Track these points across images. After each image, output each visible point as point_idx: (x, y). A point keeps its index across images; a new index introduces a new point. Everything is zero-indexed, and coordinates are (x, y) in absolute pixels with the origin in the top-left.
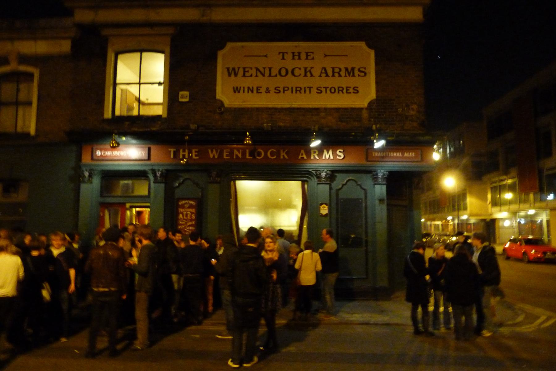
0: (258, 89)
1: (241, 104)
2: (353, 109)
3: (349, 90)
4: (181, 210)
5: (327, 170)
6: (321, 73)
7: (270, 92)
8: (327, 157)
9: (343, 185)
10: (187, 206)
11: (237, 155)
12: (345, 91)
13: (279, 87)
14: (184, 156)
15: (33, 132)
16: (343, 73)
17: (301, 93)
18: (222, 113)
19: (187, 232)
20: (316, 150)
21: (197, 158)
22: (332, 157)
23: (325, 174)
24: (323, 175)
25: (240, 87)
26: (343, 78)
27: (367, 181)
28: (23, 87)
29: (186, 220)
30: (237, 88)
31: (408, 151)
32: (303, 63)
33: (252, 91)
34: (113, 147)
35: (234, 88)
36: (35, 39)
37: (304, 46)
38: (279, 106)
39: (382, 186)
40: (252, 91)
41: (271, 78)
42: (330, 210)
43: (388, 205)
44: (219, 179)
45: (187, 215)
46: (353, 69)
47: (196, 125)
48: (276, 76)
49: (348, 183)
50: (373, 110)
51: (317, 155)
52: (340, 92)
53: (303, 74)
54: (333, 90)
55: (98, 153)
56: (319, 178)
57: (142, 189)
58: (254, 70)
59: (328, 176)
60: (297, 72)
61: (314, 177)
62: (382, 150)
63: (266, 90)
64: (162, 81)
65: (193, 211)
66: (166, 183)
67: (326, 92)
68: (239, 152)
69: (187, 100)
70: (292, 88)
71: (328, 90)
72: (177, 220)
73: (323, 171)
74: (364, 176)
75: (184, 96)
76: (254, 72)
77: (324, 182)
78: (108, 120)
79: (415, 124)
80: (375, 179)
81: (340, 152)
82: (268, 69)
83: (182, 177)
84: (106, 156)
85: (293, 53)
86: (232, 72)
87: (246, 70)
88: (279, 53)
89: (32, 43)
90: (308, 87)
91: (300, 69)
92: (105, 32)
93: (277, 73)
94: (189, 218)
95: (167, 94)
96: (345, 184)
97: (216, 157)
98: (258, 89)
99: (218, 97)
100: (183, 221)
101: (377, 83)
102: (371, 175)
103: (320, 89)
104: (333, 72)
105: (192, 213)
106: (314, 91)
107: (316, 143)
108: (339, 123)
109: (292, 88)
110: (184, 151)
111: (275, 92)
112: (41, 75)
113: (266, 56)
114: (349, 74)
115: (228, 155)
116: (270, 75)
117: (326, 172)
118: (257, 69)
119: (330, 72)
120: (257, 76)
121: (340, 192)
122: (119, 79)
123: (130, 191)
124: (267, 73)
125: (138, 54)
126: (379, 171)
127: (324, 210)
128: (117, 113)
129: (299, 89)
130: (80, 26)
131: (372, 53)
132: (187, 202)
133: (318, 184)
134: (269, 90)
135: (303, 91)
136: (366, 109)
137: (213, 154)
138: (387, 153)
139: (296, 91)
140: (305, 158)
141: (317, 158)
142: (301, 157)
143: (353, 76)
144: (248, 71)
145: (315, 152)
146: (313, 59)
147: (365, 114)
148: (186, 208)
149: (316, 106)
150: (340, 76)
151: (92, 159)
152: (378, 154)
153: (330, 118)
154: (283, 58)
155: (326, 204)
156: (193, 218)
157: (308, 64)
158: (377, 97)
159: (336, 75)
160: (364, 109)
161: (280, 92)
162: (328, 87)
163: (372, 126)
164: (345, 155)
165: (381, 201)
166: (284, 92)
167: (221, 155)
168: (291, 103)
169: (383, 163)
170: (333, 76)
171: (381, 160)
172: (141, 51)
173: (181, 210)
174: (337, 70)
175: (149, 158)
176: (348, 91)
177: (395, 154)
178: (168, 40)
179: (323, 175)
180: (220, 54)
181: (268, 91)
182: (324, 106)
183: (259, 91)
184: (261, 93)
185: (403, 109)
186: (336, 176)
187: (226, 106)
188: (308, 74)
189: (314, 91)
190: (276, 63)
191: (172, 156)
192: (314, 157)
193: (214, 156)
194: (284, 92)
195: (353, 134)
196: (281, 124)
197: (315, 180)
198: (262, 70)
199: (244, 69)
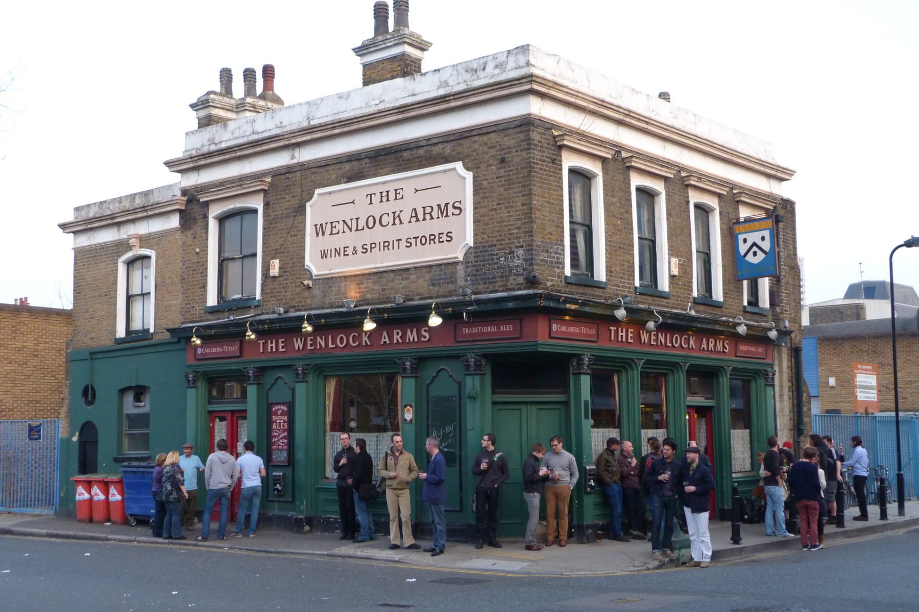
4: (274, 418)
6: (411, 217)
9: (434, 378)
10: (280, 412)
13: (366, 245)
16: (435, 214)
22: (416, 340)
29: (279, 430)
32: (391, 206)
33: (339, 254)
42: (416, 414)
45: (280, 423)
46: (447, 204)
51: (401, 337)
52: (432, 242)
54: (423, 242)
65: (285, 418)
71: (418, 240)
76: (340, 227)
81: (425, 331)
85: (381, 193)
86: (320, 230)
88: (367, 195)
90: (397, 240)
91: (388, 214)
100: (276, 432)
101: (476, 221)
104: (425, 214)
105: (284, 422)
106: (403, 243)
110: (272, 343)
113: (353, 202)
114: (442, 213)
116: (357, 230)
118: (344, 221)
119: (421, 217)
120: (344, 232)
121: (431, 387)
124: (354, 228)
126: (469, 357)
129: (386, 244)
131: (469, 176)
132: (277, 407)
135: (391, 247)
140: (388, 342)
141: (400, 341)
143: (447, 216)
144: (335, 227)
146: (402, 198)
150: (432, 218)
153: (421, 281)
154: (371, 203)
155: (411, 406)
158: (475, 243)
159: (428, 217)
162: (418, 237)
166: (371, 252)
170: (424, 219)
173: (274, 418)
174: (428, 210)
184: (348, 255)
185: (506, 259)
188: (397, 221)
189: (403, 243)
194: (371, 252)
198: (349, 222)
199: (331, 223)
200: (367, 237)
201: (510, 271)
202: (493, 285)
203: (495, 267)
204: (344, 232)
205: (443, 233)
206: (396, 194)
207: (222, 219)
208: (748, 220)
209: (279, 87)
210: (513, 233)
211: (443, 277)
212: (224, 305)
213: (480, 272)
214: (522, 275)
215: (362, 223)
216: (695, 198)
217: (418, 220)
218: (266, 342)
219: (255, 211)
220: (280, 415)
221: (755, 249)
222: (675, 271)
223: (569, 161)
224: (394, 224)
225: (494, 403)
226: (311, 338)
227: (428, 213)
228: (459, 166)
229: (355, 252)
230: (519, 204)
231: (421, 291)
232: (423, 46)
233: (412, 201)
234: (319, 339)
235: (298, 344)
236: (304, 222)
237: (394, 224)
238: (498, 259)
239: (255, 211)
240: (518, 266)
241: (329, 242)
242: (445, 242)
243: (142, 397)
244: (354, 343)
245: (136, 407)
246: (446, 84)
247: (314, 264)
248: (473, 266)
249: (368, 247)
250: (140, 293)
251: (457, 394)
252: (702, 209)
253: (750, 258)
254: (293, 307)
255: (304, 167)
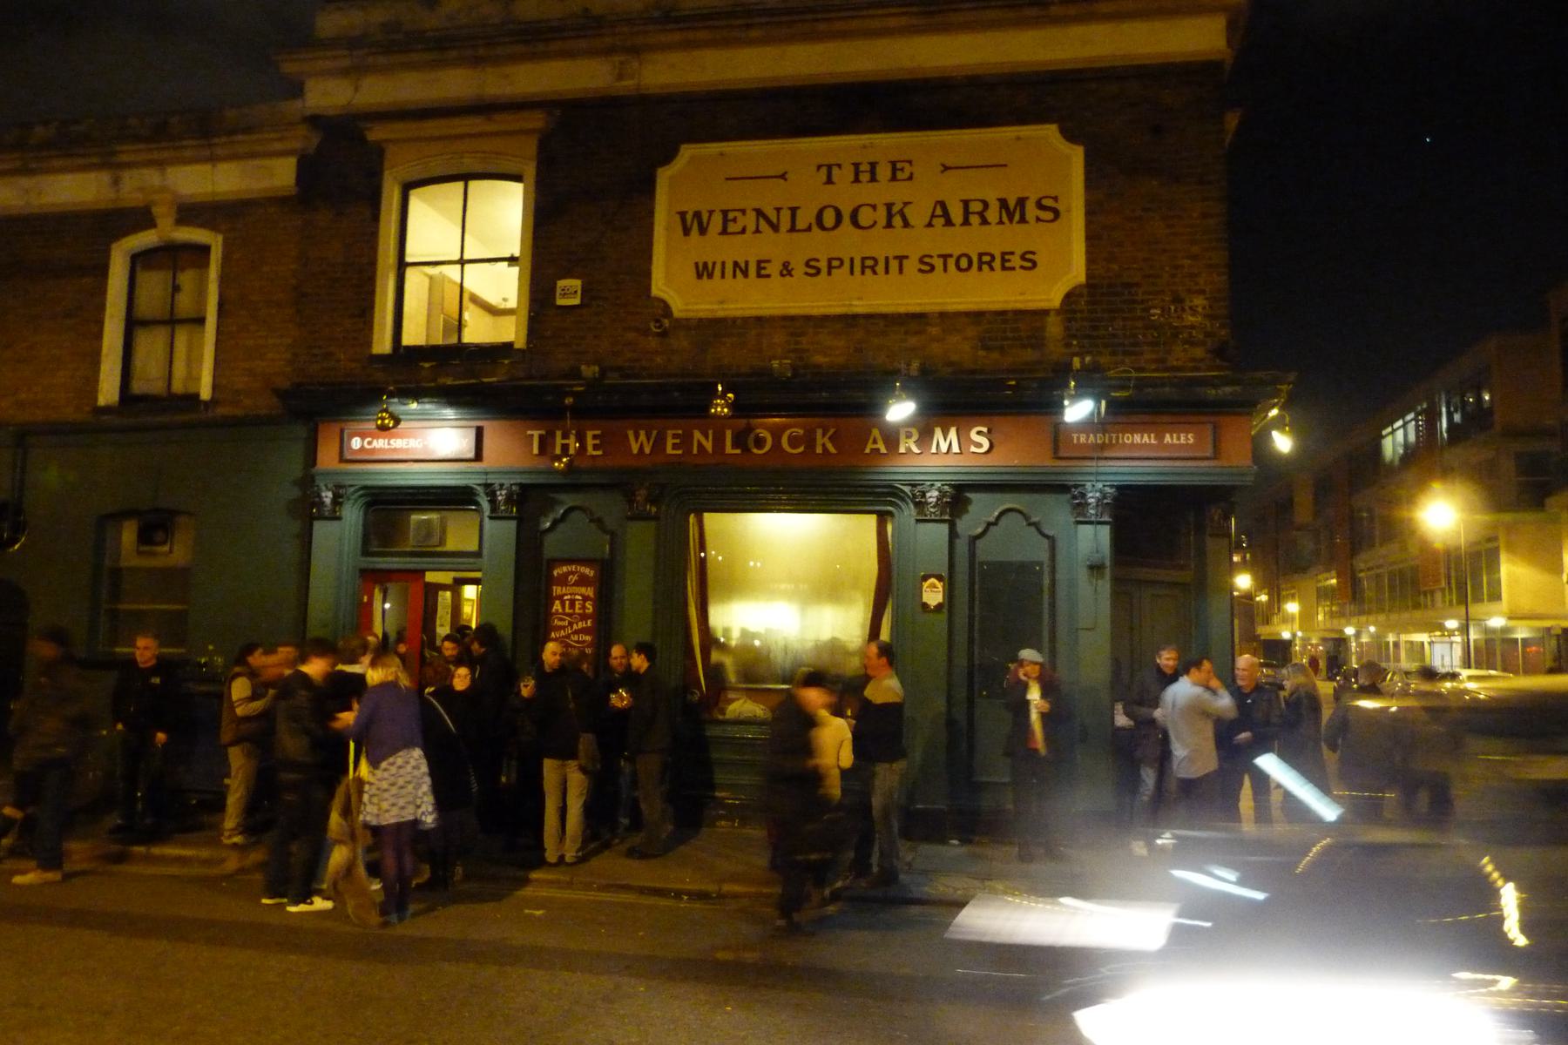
0: (760, 264)
1: (715, 307)
2: (1019, 314)
3: (1009, 261)
4: (557, 590)
5: (943, 485)
6: (933, 216)
7: (793, 272)
8: (944, 447)
10: (573, 578)
11: (700, 445)
12: (997, 264)
13: (818, 260)
14: (565, 448)
15: (205, 393)
16: (992, 215)
17: (875, 273)
18: (664, 334)
19: (571, 646)
20: (910, 429)
21: (599, 453)
22: (956, 448)
23: (936, 493)
24: (930, 497)
25: (714, 264)
26: (994, 229)
27: (1056, 514)
28: (186, 279)
29: (569, 615)
30: (705, 265)
31: (1174, 427)
32: (884, 191)
33: (745, 274)
34: (383, 428)
35: (697, 264)
36: (213, 159)
37: (886, 144)
38: (815, 312)
39: (1099, 527)
40: (745, 274)
41: (795, 235)
42: (950, 594)
43: (1117, 581)
44: (654, 509)
46: (1021, 202)
47: (597, 369)
48: (809, 229)
49: (1004, 521)
50: (1079, 315)
52: (985, 267)
53: (883, 221)
54: (964, 263)
55: (356, 443)
56: (920, 505)
57: (460, 533)
58: (752, 216)
59: (945, 500)
60: (865, 217)
61: (907, 504)
62: (1087, 426)
63: (781, 268)
64: (517, 254)
65: (589, 592)
66: (520, 520)
67: (945, 269)
68: (707, 438)
69: (576, 301)
70: (852, 260)
71: (951, 262)
72: (549, 615)
73: (932, 485)
74: (1050, 499)
75: (569, 292)
76: (750, 220)
77: (933, 517)
78: (382, 358)
79: (1199, 352)
80: (1080, 506)
81: (979, 433)
82: (789, 212)
83: (561, 503)
84: (373, 451)
85: (856, 165)
86: (695, 223)
87: (731, 215)
88: (819, 167)
89: (204, 169)
90: (896, 258)
91: (874, 207)
92: (376, 134)
93: (813, 221)
94: (577, 611)
95: (527, 289)
96: (995, 523)
97: (647, 450)
98: (760, 264)
99: (656, 291)
101: (1091, 238)
102: (1069, 496)
103: (927, 260)
104: (967, 213)
105: (585, 598)
106: (911, 265)
107: (900, 410)
108: (981, 353)
109: (852, 260)
110: (565, 436)
111: (806, 274)
112: (227, 246)
113: (783, 176)
115: (677, 444)
116: (793, 229)
117: (939, 490)
118: (760, 213)
119: (956, 214)
120: (757, 231)
121: (979, 543)
122: (416, 249)
123: (435, 540)
125: (460, 185)
126: (1089, 485)
127: (933, 595)
128: (413, 335)
129: (869, 263)
130: (315, 121)
131: (1077, 155)
133: (918, 521)
134: (790, 268)
135: (880, 268)
136: (1058, 312)
137: (638, 442)
138: (1114, 435)
139: (863, 268)
140: (883, 450)
141: (915, 450)
142: (872, 449)
144: (735, 220)
145: (909, 436)
146: (910, 178)
147: (1054, 328)
148: (570, 586)
149: (918, 309)
150: (985, 222)
151: (342, 460)
152: (1087, 440)
153: (954, 339)
154: (829, 181)
155: (940, 578)
156: (587, 611)
157: (898, 193)
158: (1089, 276)
159: (975, 219)
160: (1052, 313)
161: (818, 271)
162: (951, 256)
163: (1072, 360)
164: (993, 441)
165: (1095, 568)
166: (829, 273)
167: (659, 444)
168: (847, 303)
169: (1102, 463)
170: (966, 222)
171: (1095, 455)
172: (466, 178)
173: (557, 590)
174: (976, 207)
175: (478, 456)
176: (1007, 265)
177: (1137, 438)
178: (531, 146)
179: (930, 497)
180: (664, 176)
181: (786, 270)
182: (938, 309)
183: (763, 272)
184: (768, 276)
186: (968, 501)
187: (676, 314)
188: (897, 221)
190: (809, 194)
191: (536, 451)
192: (909, 450)
193: (641, 448)
194: (829, 273)
195: (1013, 383)
196: (819, 359)
197: (910, 511)
199: (725, 213)
201: (1175, 336)
202: (1133, 358)
203: (1139, 324)
204: (757, 231)
205: (1012, 253)
206: (894, 170)
210: (1183, 266)
211: (1010, 335)
213: (1102, 332)
214: (1203, 343)
217: (949, 222)
218: (551, 434)
220: (573, 585)
224: (889, 225)
226: (674, 432)
229: (786, 270)
230: (1195, 215)
231: (955, 358)
234: (697, 435)
235: (702, 440)
237: (889, 225)
238: (1147, 310)
240: (1193, 327)
242: (1018, 270)
243: (159, 536)
244: (793, 446)
245: (140, 553)
248: (1083, 319)
249: (823, 265)
250: (167, 317)
251: (1044, 556)
254: (619, 369)
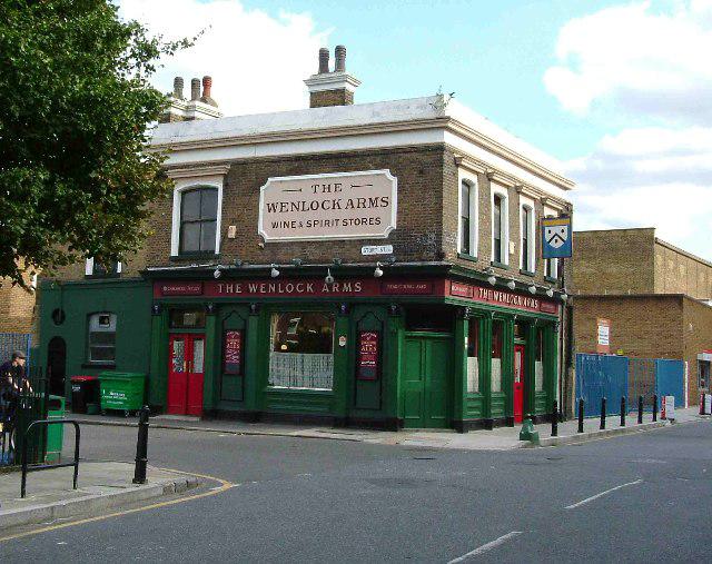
32: (331, 196)
86: (271, 208)
106: (340, 223)
124: (301, 208)
131: (395, 180)
137: (253, 289)
189: (340, 223)
198: (296, 204)
200: (311, 216)
207: (184, 193)
208: (550, 218)
209: (214, 93)
212: (184, 255)
215: (307, 206)
216: (523, 201)
219: (216, 189)
221: (556, 238)
222: (512, 252)
223: (463, 174)
225: (407, 337)
227: (362, 204)
228: (387, 172)
232: (356, 83)
233: (346, 194)
236: (258, 201)
239: (216, 189)
241: (279, 217)
246: (375, 114)
247: (265, 231)
252: (526, 209)
253: (553, 244)
255: (257, 161)
